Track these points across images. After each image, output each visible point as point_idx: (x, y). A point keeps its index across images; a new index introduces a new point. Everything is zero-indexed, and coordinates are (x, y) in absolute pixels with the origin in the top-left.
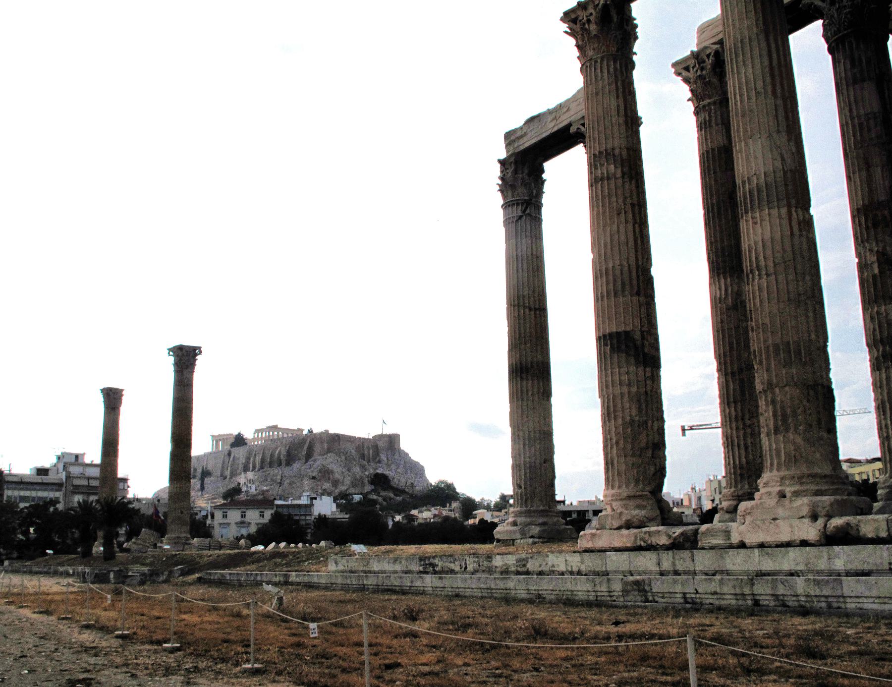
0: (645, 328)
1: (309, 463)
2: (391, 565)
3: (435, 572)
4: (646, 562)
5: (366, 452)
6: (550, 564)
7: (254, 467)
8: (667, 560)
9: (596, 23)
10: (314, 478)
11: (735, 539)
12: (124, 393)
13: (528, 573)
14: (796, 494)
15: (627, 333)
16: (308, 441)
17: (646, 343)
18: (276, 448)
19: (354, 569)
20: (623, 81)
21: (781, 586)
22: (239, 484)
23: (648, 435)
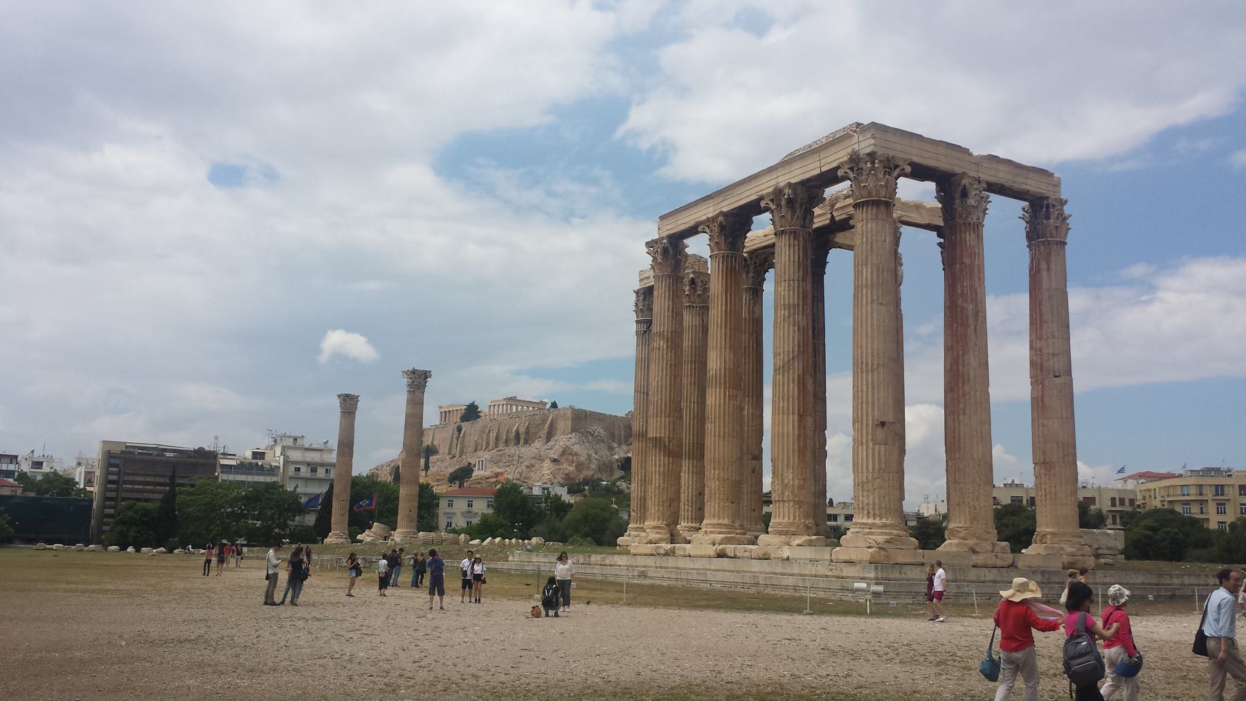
0: (671, 436)
4: (651, 561)
5: (616, 432)
7: (488, 444)
8: (660, 561)
9: (661, 255)
10: (555, 461)
11: (687, 553)
12: (359, 398)
13: (605, 565)
14: (711, 532)
15: (660, 438)
16: (550, 418)
17: (671, 444)
20: (673, 290)
22: (470, 464)
23: (667, 494)
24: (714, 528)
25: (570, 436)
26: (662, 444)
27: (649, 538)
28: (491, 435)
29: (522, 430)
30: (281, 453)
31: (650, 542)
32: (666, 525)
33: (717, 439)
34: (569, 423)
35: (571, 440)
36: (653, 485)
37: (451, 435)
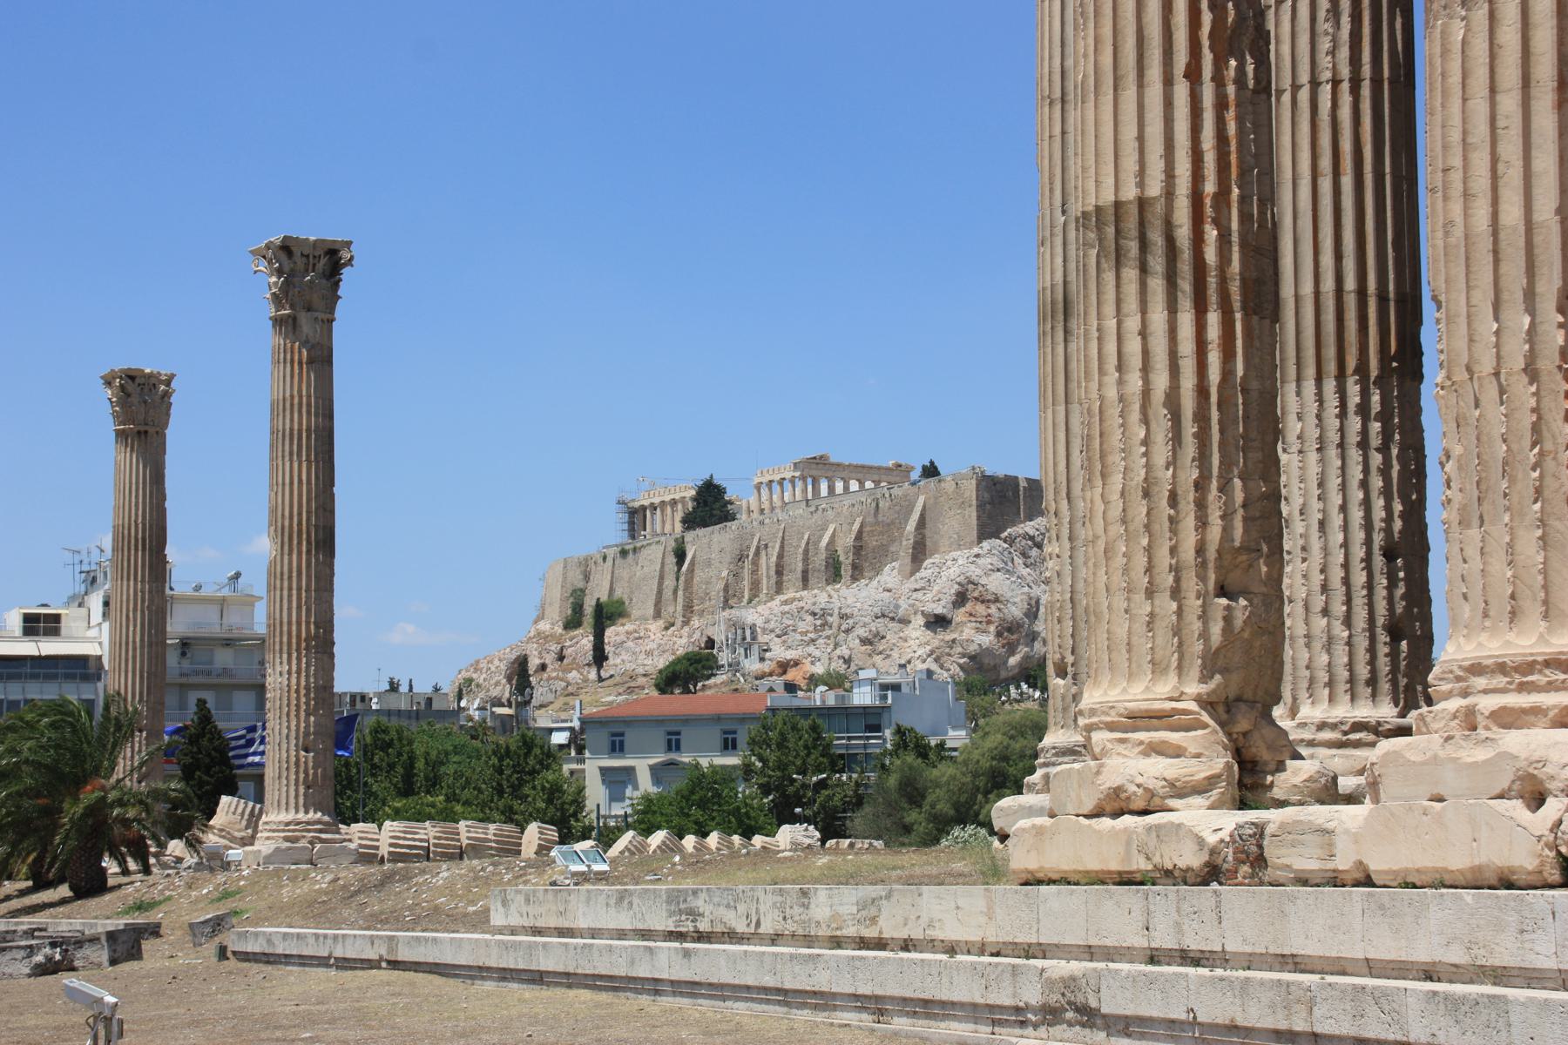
1: (923, 573)
2: (612, 911)
3: (701, 937)
6: (924, 921)
10: (938, 622)
11: (1343, 862)
12: (173, 385)
13: (880, 944)
15: (1142, 203)
18: (825, 529)
19: (540, 923)
21: (1372, 1011)
22: (711, 643)
23: (1202, 523)
24: (1522, 688)
25: (976, 550)
26: (1157, 238)
27: (1109, 780)
28: (763, 560)
29: (846, 541)
30: (104, 615)
31: (1116, 805)
32: (1207, 703)
33: (1509, 103)
34: (972, 513)
35: (980, 561)
36: (1117, 480)
37: (658, 567)
